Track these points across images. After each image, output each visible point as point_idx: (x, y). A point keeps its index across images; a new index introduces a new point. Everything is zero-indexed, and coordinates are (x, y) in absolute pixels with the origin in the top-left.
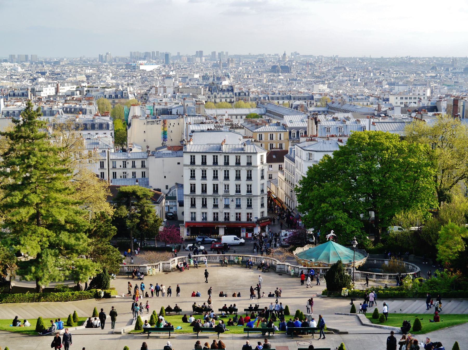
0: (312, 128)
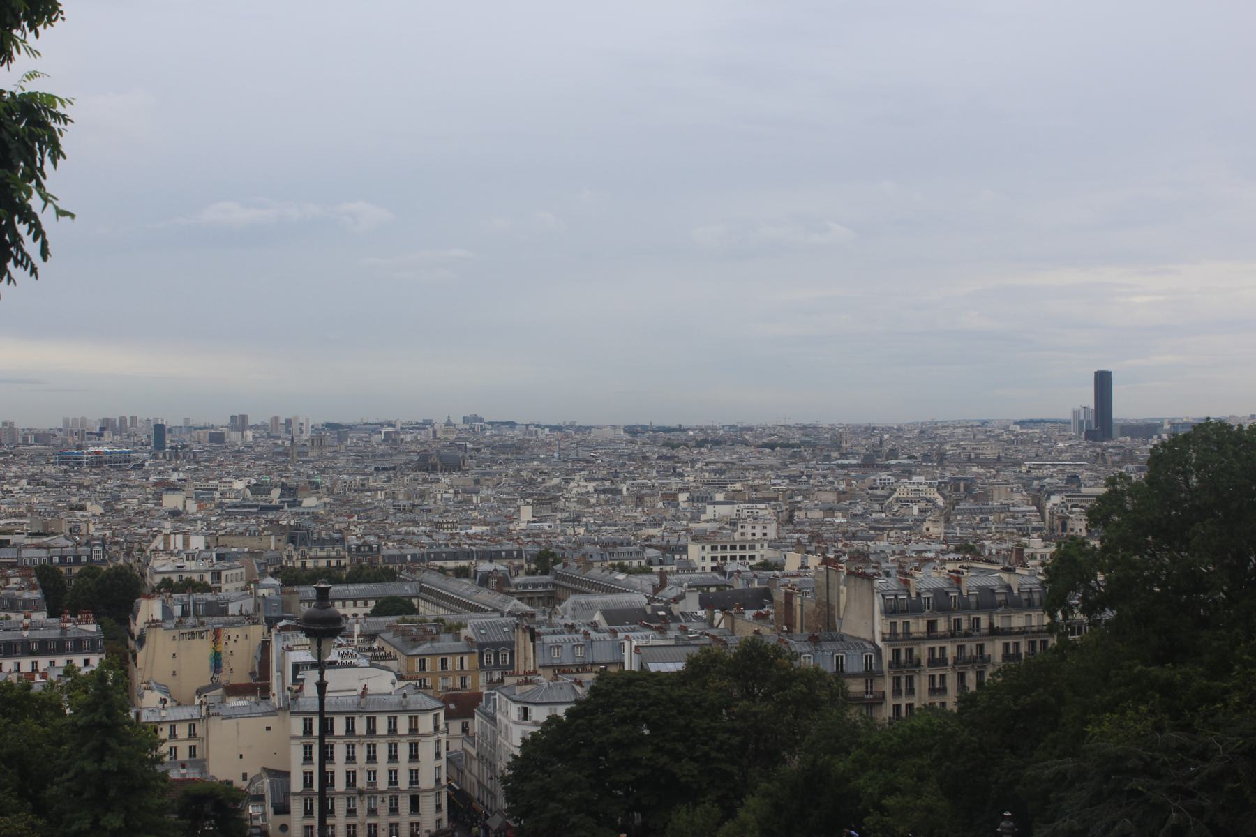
0: (525, 647)
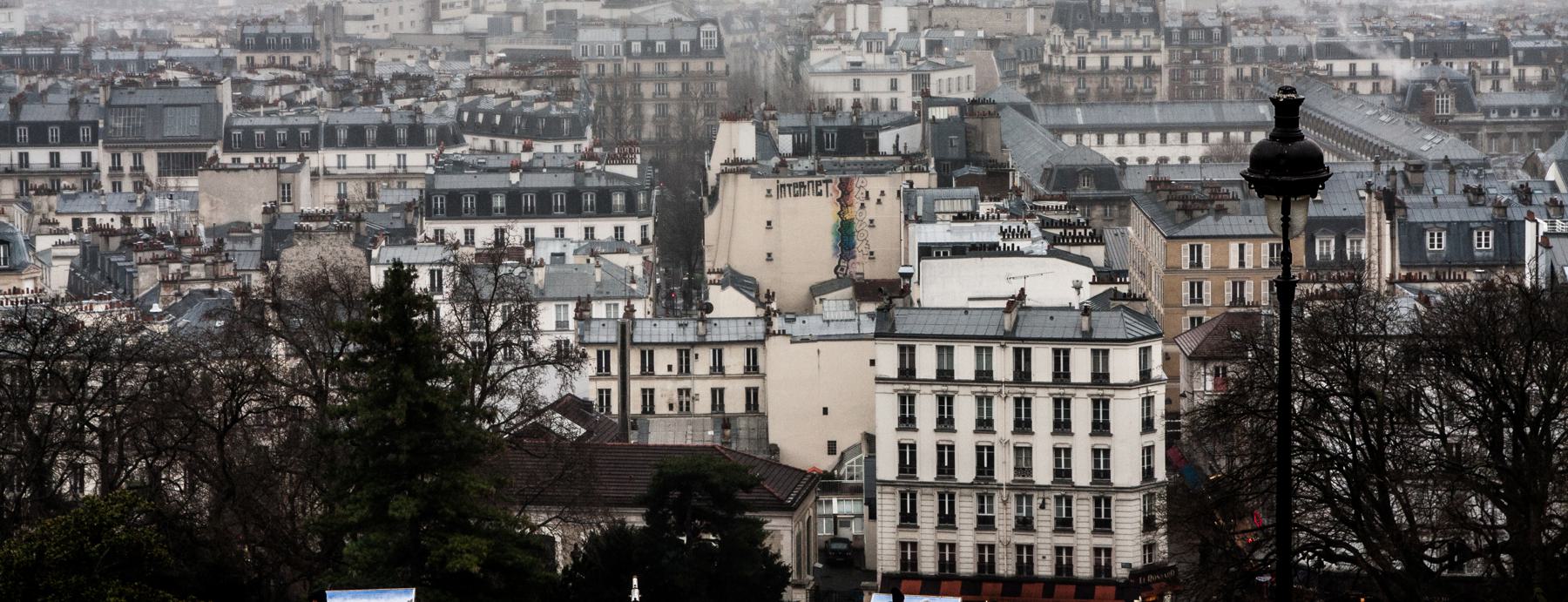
0: (1379, 228)
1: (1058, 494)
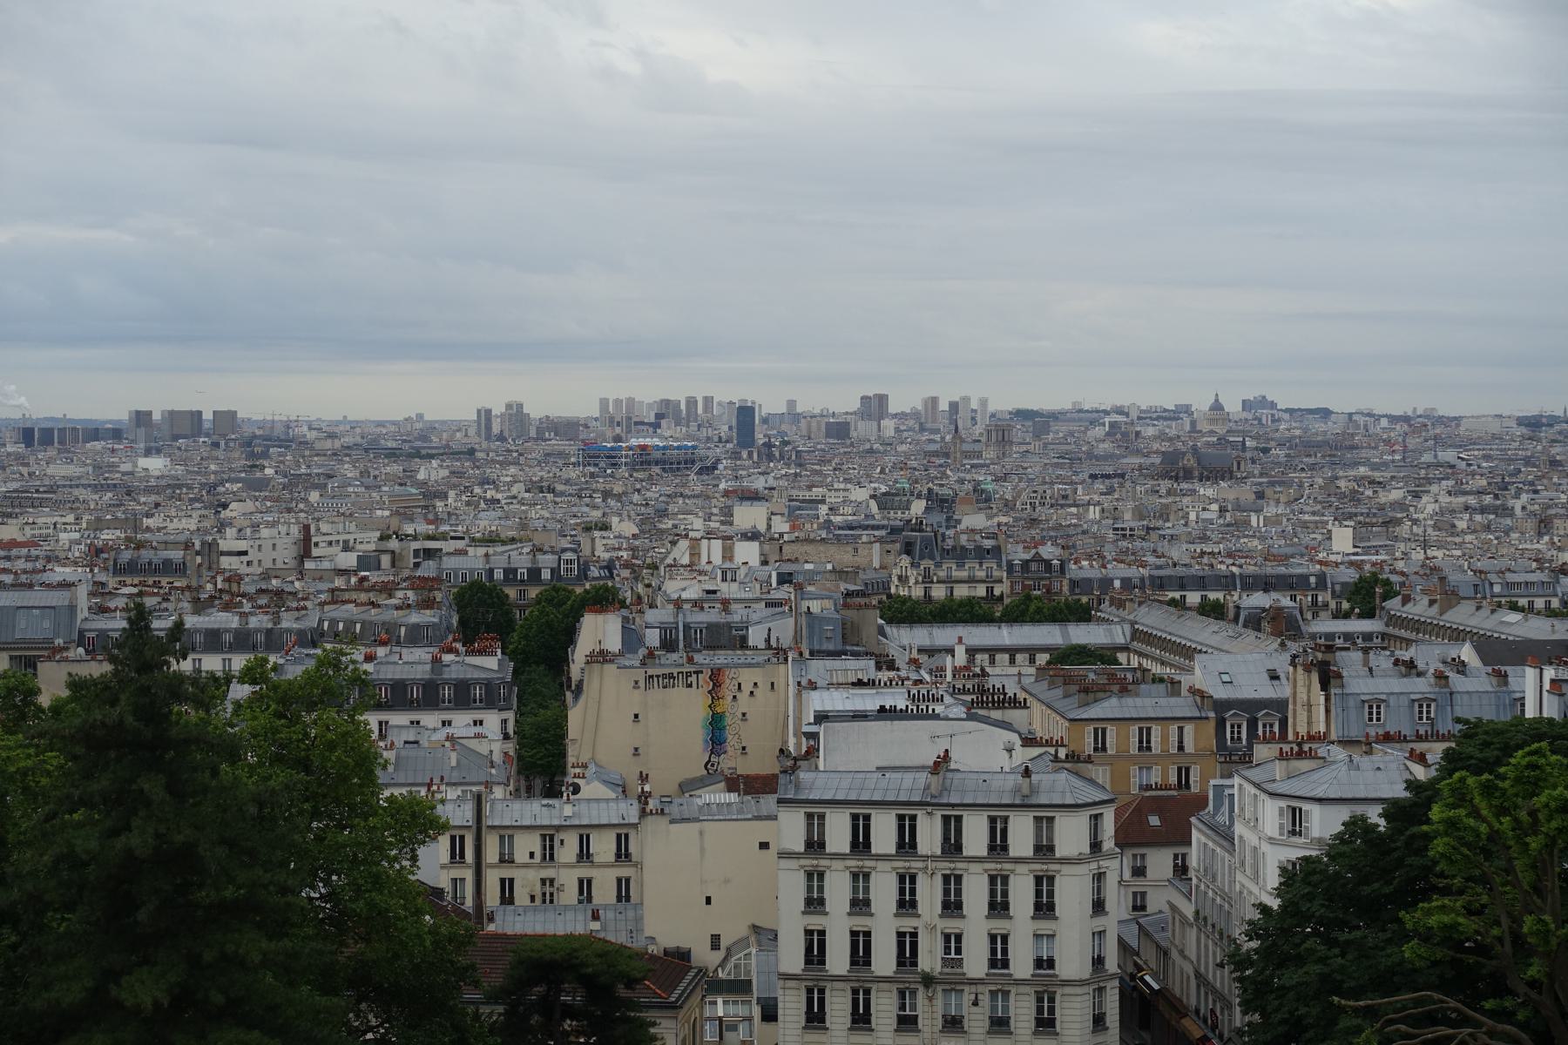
1: (993, 988)
